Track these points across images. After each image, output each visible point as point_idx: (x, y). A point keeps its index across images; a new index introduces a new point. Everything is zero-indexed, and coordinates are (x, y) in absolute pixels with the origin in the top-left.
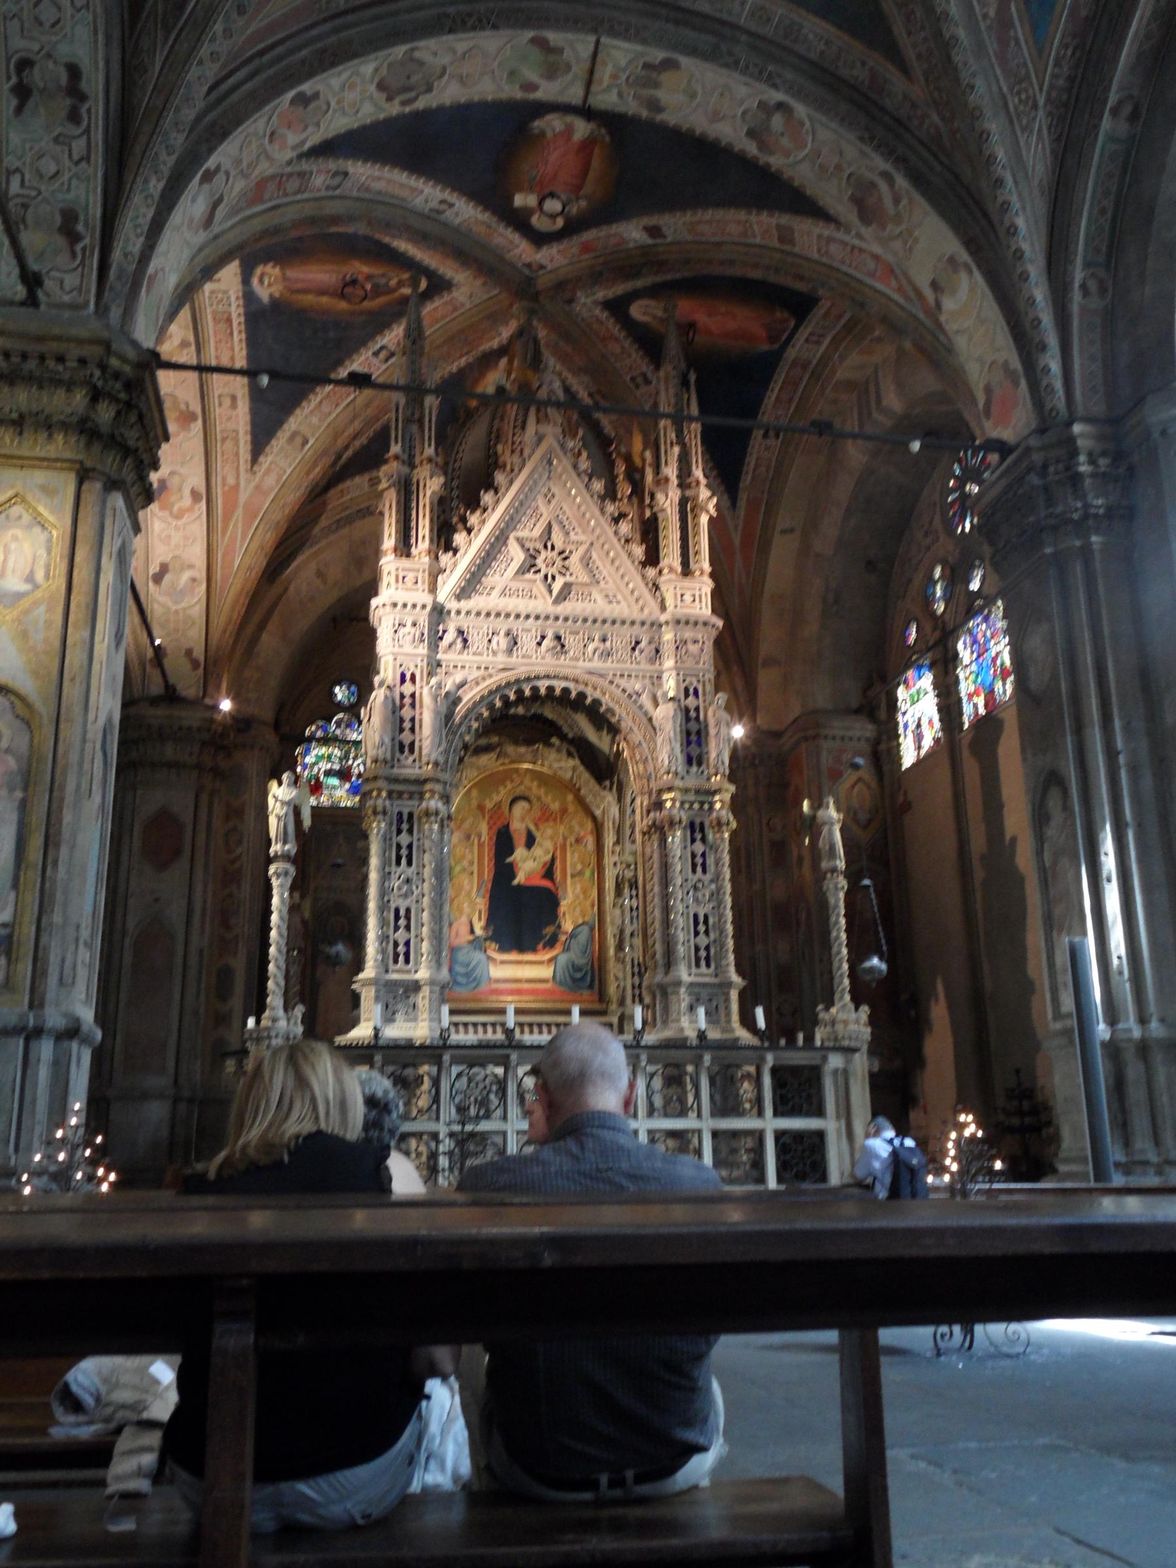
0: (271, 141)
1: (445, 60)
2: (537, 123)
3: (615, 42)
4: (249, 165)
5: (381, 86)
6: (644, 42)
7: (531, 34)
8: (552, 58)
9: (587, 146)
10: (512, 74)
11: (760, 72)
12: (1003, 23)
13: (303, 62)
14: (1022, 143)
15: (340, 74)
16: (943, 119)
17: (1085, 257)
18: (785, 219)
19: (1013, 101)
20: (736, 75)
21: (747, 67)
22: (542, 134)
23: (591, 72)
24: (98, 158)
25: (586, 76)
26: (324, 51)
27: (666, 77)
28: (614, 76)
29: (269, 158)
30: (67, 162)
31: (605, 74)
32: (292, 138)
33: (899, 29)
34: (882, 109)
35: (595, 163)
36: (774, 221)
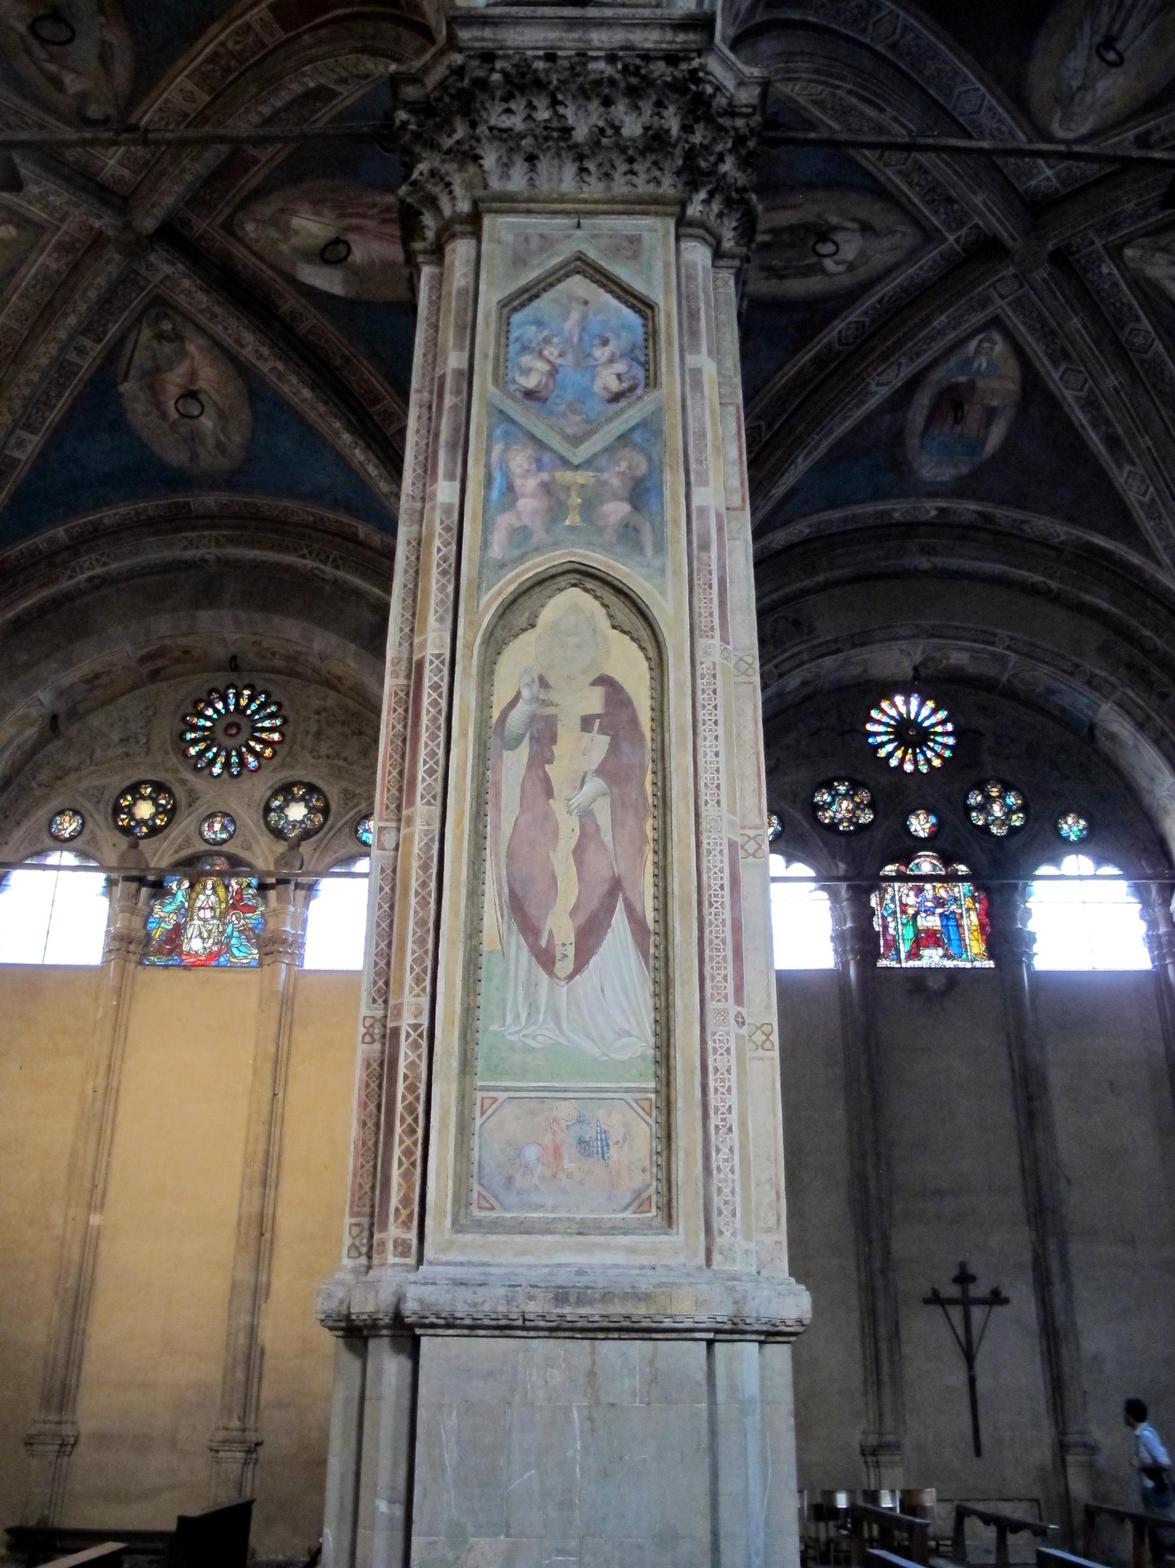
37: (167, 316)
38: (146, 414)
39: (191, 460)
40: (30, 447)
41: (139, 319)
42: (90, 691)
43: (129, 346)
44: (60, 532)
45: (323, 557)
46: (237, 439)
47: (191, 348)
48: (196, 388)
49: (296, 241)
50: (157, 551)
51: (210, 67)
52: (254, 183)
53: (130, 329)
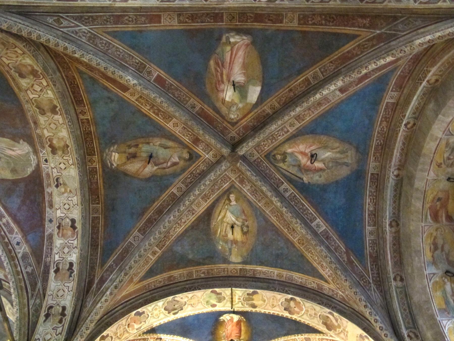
0: (128, 327)
1: (186, 300)
2: (221, 318)
3: (237, 289)
4: (120, 335)
5: (165, 309)
6: (246, 288)
7: (211, 290)
8: (219, 296)
9: (239, 323)
10: (207, 302)
11: (283, 290)
12: (350, 262)
13: (140, 303)
14: (369, 294)
15: (151, 306)
16: (343, 292)
17: (405, 326)
18: (306, 336)
19: (362, 283)
20: (276, 293)
21: (279, 290)
22: (224, 321)
23: (232, 298)
24: (64, 333)
25: (231, 300)
26: (147, 300)
27: (255, 297)
28: (239, 299)
29: (128, 332)
30: (55, 335)
31: (236, 299)
32: (136, 326)
33: (321, 271)
34: (324, 294)
35: (243, 328)
36: (303, 337)
37: (274, 156)
38: (320, 177)
39: (347, 166)
40: (321, 223)
41: (275, 166)
42: (442, 250)
43: (287, 173)
44: (368, 229)
45: (401, 121)
46: (337, 145)
47: (289, 151)
48: (309, 154)
49: (237, 101)
50: (389, 193)
51: (160, 115)
52: (211, 111)
53: (279, 171)
